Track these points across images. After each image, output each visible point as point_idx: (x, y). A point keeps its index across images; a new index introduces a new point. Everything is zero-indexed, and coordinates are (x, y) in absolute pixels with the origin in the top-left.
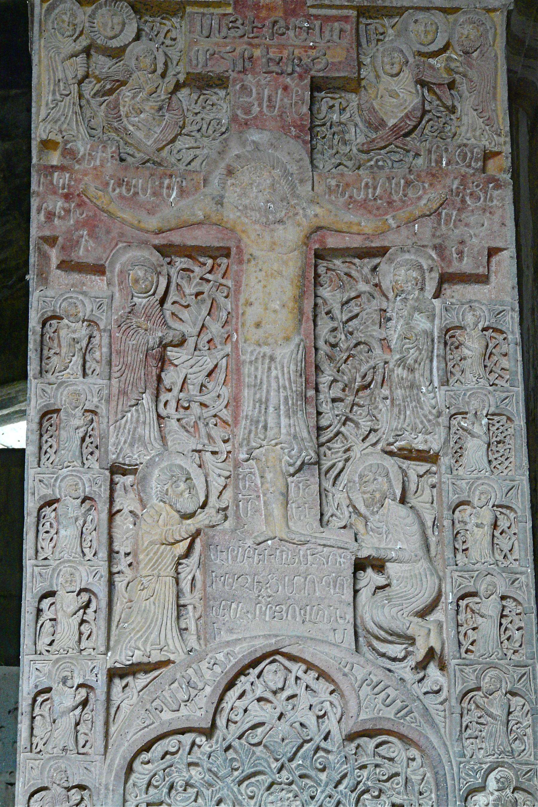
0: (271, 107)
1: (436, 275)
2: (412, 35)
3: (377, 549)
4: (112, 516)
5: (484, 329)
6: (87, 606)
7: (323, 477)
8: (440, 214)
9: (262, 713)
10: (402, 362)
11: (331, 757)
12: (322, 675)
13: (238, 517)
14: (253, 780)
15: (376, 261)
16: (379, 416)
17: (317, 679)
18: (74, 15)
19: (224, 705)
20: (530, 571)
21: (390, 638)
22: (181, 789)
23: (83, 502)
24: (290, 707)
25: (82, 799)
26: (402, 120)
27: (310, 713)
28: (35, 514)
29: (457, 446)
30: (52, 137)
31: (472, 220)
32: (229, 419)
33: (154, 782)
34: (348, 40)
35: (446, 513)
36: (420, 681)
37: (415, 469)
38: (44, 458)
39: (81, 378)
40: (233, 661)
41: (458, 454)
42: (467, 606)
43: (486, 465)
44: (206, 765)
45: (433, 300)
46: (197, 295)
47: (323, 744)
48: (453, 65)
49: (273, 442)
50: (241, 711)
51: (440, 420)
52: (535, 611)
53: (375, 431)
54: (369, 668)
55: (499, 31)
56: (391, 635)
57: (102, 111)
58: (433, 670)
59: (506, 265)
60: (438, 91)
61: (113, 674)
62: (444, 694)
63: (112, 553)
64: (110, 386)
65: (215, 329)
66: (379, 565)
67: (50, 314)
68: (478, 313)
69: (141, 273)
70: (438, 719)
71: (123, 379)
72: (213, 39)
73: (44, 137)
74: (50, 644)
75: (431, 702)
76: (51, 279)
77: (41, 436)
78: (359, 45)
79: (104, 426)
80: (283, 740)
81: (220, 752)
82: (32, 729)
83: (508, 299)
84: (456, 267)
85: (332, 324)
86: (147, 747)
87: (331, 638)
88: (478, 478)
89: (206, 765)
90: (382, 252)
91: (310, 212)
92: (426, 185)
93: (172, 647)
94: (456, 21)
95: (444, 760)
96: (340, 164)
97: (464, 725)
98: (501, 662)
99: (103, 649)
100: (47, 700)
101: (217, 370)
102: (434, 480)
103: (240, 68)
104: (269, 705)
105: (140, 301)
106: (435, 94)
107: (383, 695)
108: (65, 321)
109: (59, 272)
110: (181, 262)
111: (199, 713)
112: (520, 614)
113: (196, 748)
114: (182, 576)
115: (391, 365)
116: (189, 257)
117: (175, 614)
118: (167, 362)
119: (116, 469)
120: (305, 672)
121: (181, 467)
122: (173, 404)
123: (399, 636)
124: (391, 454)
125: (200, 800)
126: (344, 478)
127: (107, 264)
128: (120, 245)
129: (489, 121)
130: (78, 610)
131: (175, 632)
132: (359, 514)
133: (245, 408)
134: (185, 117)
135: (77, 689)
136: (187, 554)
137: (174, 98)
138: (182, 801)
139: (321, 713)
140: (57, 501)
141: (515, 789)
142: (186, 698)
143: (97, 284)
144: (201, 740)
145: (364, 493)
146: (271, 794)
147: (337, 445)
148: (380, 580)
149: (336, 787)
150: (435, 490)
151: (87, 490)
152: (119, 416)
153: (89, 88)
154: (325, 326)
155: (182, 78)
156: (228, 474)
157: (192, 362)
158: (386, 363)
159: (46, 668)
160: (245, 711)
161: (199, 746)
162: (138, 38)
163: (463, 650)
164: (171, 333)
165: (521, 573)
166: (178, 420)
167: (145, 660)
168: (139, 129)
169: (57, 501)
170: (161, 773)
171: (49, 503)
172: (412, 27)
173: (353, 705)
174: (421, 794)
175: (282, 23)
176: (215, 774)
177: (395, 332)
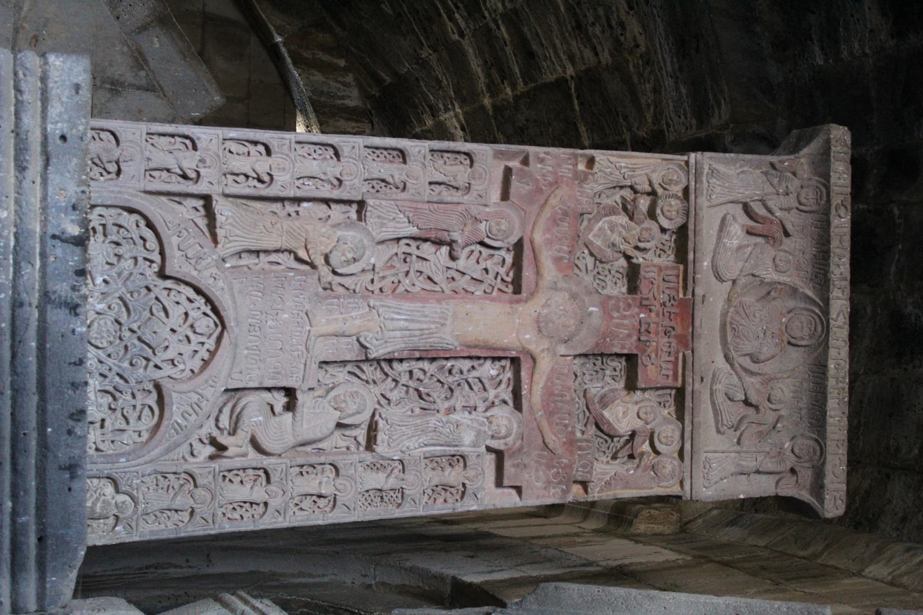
0: (618, 326)
1: (502, 447)
2: (665, 427)
3: (303, 406)
4: (327, 202)
5: (464, 485)
7: (355, 364)
9: (176, 316)
11: (141, 371)
12: (206, 363)
13: (326, 298)
14: (124, 309)
15: (511, 403)
16: (399, 406)
17: (203, 360)
18: (677, 183)
20: (286, 525)
21: (234, 416)
22: (116, 251)
23: (338, 179)
24: (181, 338)
25: (109, 173)
27: (176, 354)
28: (329, 142)
29: (378, 465)
30: (597, 165)
31: (541, 473)
32: (398, 291)
33: (122, 230)
34: (662, 382)
35: (330, 459)
36: (201, 440)
37: (361, 434)
38: (369, 151)
39: (429, 180)
40: (218, 293)
41: (374, 467)
42: (259, 476)
43: (366, 489)
44: (136, 271)
45: (484, 447)
46: (486, 270)
47: (151, 364)
48: (645, 457)
49: (382, 325)
50: (177, 299)
52: (256, 529)
53: (389, 404)
54: (212, 400)
55: (668, 490)
56: (237, 417)
58: (210, 450)
59: (507, 500)
60: (627, 447)
61: (207, 199)
62: (191, 459)
63: (298, 200)
64: (424, 202)
65: (463, 282)
66: (290, 406)
67: (474, 158)
69: (503, 227)
70: (172, 455)
71: (427, 212)
72: (662, 284)
73: (597, 159)
74: (230, 152)
75: (185, 448)
78: (657, 389)
79: (394, 197)
81: (144, 283)
82: (164, 135)
83: (486, 502)
85: (465, 370)
86: (150, 225)
87: (235, 370)
88: (356, 482)
89: (136, 271)
90: (518, 406)
94: (674, 458)
95: (141, 460)
96: (576, 376)
97: (167, 475)
98: (217, 505)
99: (227, 191)
100: (187, 147)
101: (433, 285)
102: (353, 448)
103: (645, 302)
104: (182, 321)
105: (483, 226)
106: (625, 445)
108: (469, 170)
109: (503, 167)
110: (509, 259)
111: (177, 266)
112: (253, 516)
113: (148, 263)
114: (281, 255)
115: (438, 415)
116: (513, 264)
117: (253, 248)
119: (361, 205)
120: (208, 350)
121: (362, 256)
122: (408, 250)
123: (236, 423)
124: (373, 415)
125: (107, 267)
126: (355, 379)
127: (509, 202)
128: (523, 213)
129: (608, 483)
130: (257, 174)
131: (239, 249)
132: (328, 391)
134: (607, 263)
135: (196, 171)
137: (621, 255)
138: (107, 252)
139: (176, 363)
140: (339, 160)
141: (117, 517)
142: (189, 256)
143: (495, 195)
145: (345, 396)
147: (379, 375)
148: (278, 408)
149: (118, 374)
150: (345, 449)
151: (347, 183)
152: (402, 209)
153: (628, 193)
154: (466, 365)
155: (634, 261)
156: (357, 291)
157: (439, 266)
158: (438, 411)
159: (214, 146)
160: (178, 303)
161: (150, 266)
163: (226, 474)
164: (459, 249)
165: (285, 517)
166: (396, 254)
167: (218, 224)
169: (339, 160)
170: (129, 236)
171: (337, 154)
172: (671, 427)
173: (184, 387)
174: (113, 442)
176: (127, 279)
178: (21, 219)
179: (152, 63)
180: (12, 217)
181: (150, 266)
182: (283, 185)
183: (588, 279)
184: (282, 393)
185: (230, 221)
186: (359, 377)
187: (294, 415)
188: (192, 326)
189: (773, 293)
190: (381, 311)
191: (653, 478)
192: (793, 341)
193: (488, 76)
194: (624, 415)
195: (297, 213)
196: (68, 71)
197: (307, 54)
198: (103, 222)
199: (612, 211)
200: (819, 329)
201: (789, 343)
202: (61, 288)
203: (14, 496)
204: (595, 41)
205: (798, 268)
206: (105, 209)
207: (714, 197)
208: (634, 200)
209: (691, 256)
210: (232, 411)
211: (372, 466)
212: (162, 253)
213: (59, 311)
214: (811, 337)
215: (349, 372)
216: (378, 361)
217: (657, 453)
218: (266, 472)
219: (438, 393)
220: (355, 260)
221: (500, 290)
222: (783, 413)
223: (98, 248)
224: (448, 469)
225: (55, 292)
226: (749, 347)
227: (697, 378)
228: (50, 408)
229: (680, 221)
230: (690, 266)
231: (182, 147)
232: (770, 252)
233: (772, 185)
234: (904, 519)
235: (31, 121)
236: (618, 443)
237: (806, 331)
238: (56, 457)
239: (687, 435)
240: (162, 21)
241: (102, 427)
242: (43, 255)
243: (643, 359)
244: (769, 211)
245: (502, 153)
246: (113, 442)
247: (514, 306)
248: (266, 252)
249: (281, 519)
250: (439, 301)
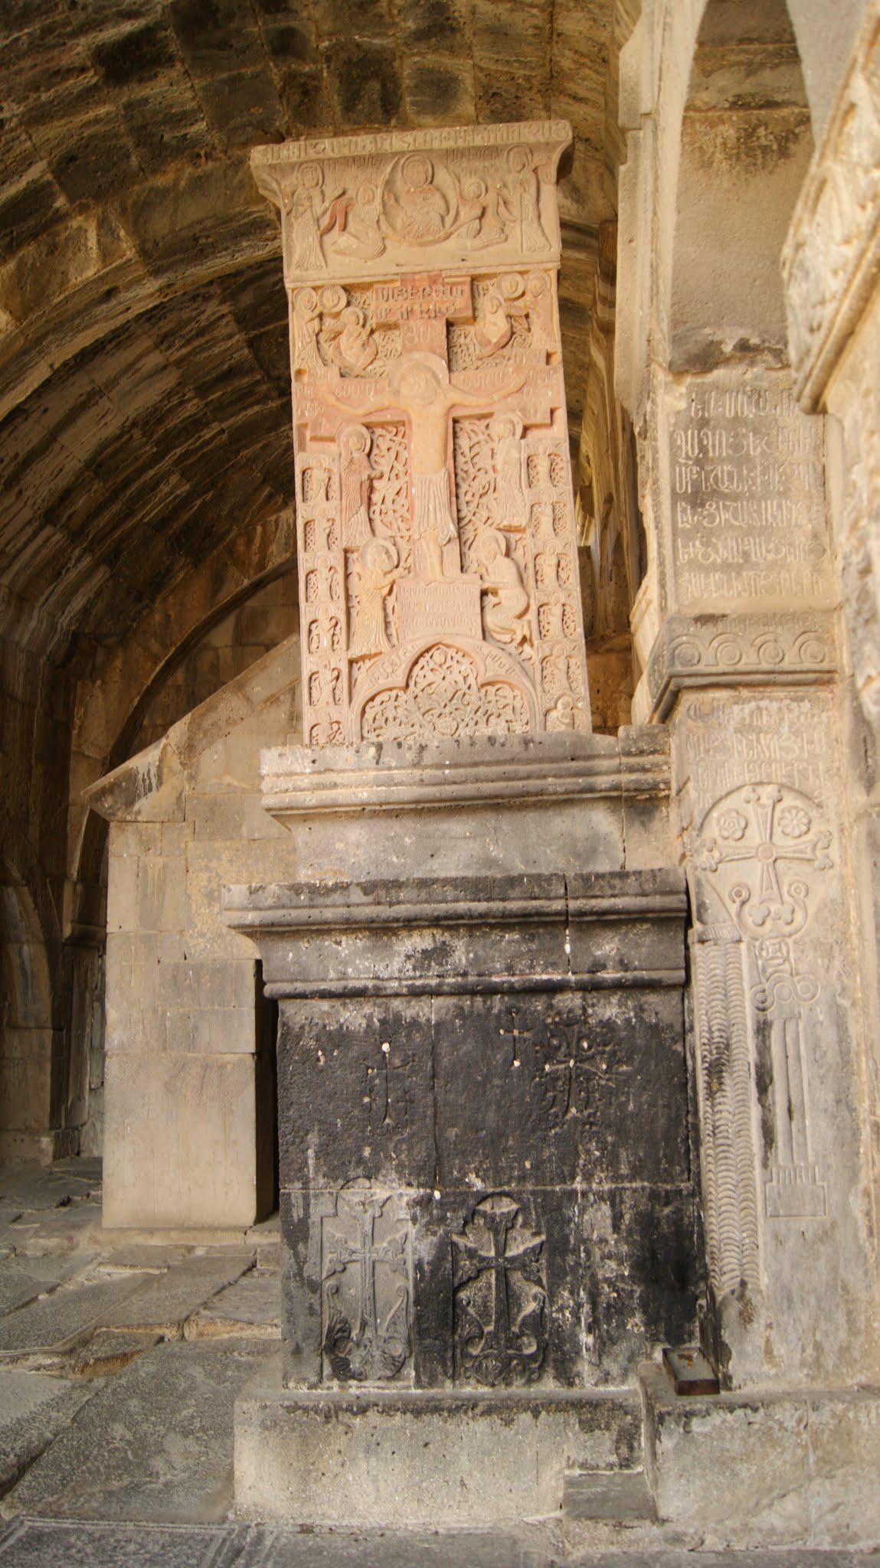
4: (347, 576)
15: (487, 421)
20: (579, 589)
41: (537, 527)
58: (526, 647)
63: (348, 597)
65: (398, 467)
70: (530, 673)
86: (372, 699)
90: (490, 415)
105: (356, 455)
110: (379, 431)
124: (499, 530)
143: (333, 447)
144: (401, 693)
147: (470, 527)
153: (322, 337)
154: (461, 459)
175: (428, 289)
177: (499, 462)
179: (274, 691)
182: (338, 610)
193: (251, 405)
194: (493, 325)
196: (271, 761)
197: (256, 559)
202: (410, 756)
203: (545, 777)
204: (213, 318)
212: (390, 689)
214: (424, 163)
217: (523, 294)
219: (482, 480)
220: (387, 552)
223: (390, 732)
224: (539, 468)
228: (488, 758)
229: (342, 292)
234: (595, 20)
235: (305, 782)
236: (518, 328)
237: (421, 168)
239: (509, 269)
240: (240, 687)
242: (390, 768)
243: (449, 315)
248: (386, 616)
250: (412, 485)
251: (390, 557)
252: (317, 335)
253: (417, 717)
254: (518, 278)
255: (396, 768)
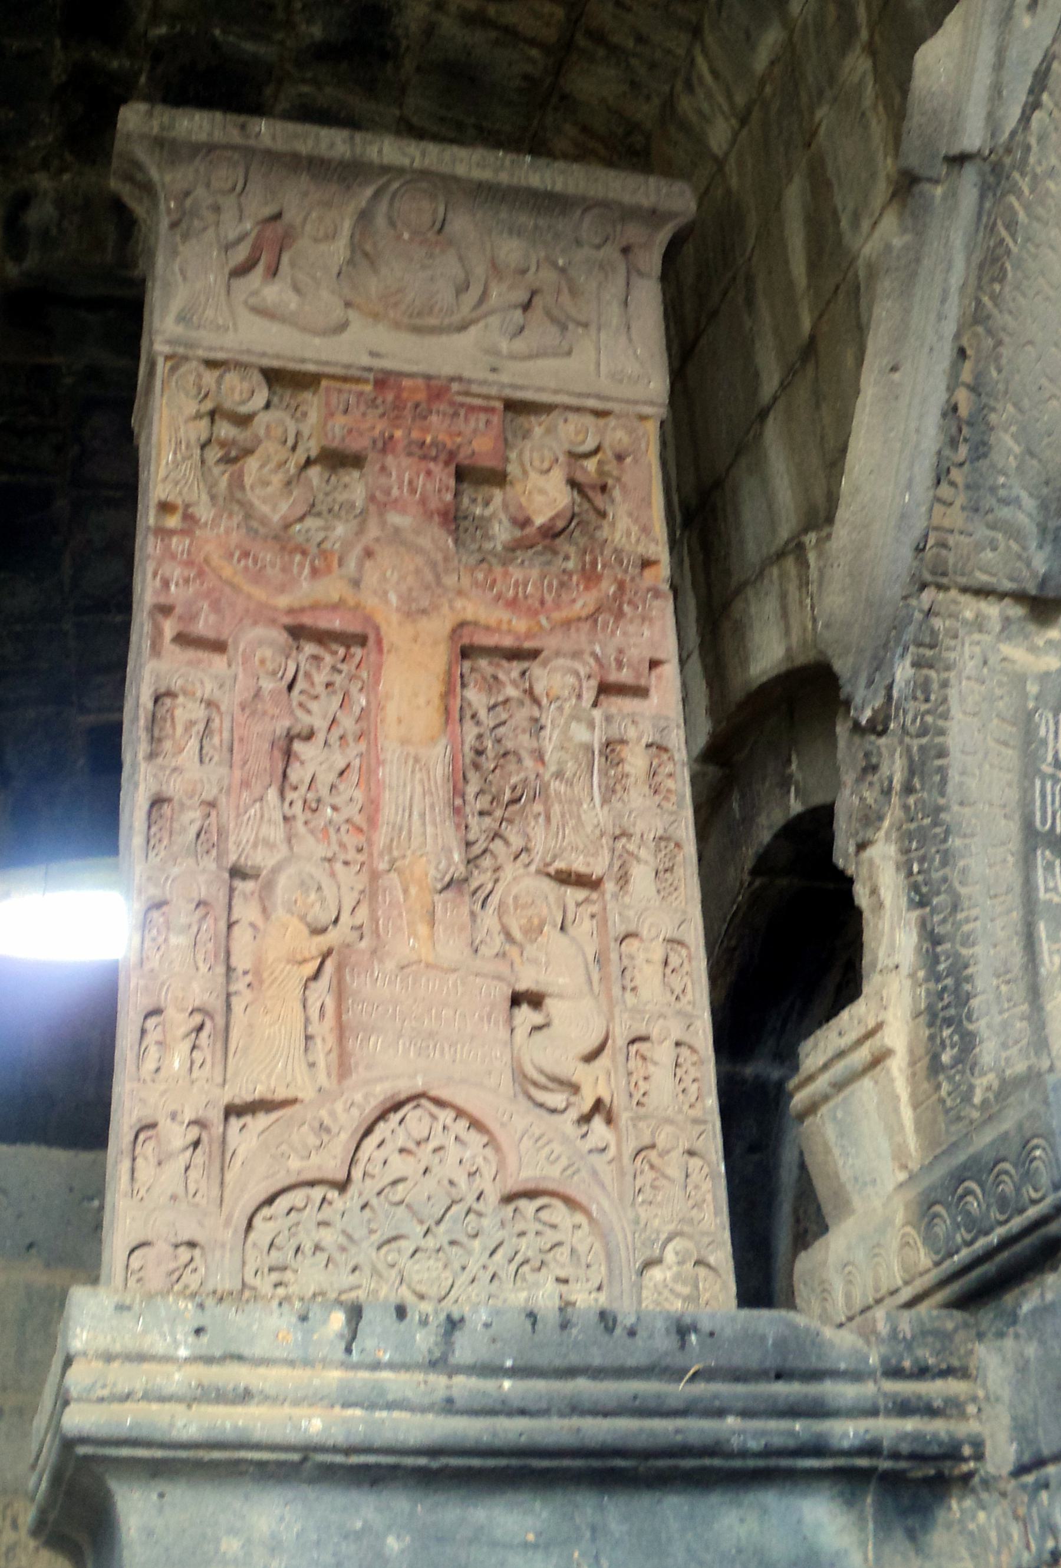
0: (413, 490)
1: (594, 683)
4: (230, 926)
5: (649, 746)
6: (200, 1028)
8: (596, 621)
10: (559, 775)
11: (485, 1222)
12: (475, 1124)
14: (394, 1245)
15: (525, 665)
18: (199, 376)
19: (360, 1154)
24: (437, 1160)
25: (192, 1260)
26: (553, 519)
29: (621, 872)
31: (631, 629)
37: (573, 895)
38: (152, 855)
40: (373, 1102)
41: (623, 879)
46: (328, 685)
47: (475, 1206)
49: (419, 853)
51: (604, 840)
57: (224, 482)
58: (598, 1122)
62: (612, 1152)
65: (347, 723)
66: (535, 1000)
68: (641, 727)
70: (608, 1181)
73: (163, 497)
75: (595, 1158)
76: (163, 653)
77: (149, 827)
80: (429, 1198)
82: (133, 1171)
84: (614, 677)
86: (270, 1201)
89: (339, 1224)
90: (534, 654)
91: (459, 604)
92: (582, 587)
93: (300, 1082)
94: (606, 425)
99: (220, 1080)
100: (150, 1138)
102: (594, 908)
103: (380, 444)
104: (410, 1159)
107: (546, 1151)
108: (181, 699)
110: (310, 648)
113: (325, 1205)
114: (310, 1002)
118: (292, 759)
122: (298, 806)
124: (548, 875)
126: (494, 900)
127: (230, 640)
129: (646, 530)
131: (304, 1066)
133: (386, 811)
136: (316, 976)
137: (303, 475)
142: (318, 1143)
144: (333, 1194)
146: (417, 1262)
147: (487, 862)
148: (537, 1018)
152: (242, 810)
155: (314, 453)
162: (268, 406)
167: (269, 1096)
168: (264, 502)
170: (286, 1232)
173: (512, 1160)
174: (588, 1266)
177: (550, 740)
178: (321, 1399)
180: (318, 1410)
181: (330, 1203)
183: (340, 529)
184: (516, 1011)
185: (263, 1077)
186: (491, 892)
187: (550, 995)
188: (418, 1143)
189: (368, 247)
190: (396, 853)
191: (636, 461)
192: (438, 225)
195: (245, 973)
198: (266, 1270)
199: (237, 482)
200: (424, 185)
201: (440, 231)
202: (424, 1341)
205: (328, 205)
206: (247, 1268)
207: (221, 322)
208: (223, 444)
209: (311, 368)
210: (544, 1088)
211: (622, 882)
212: (312, 1184)
213: (457, 1346)
214: (433, 197)
215: (483, 906)
216: (469, 862)
217: (597, 451)
218: (633, 1042)
220: (319, 888)
221: (358, 666)
222: (542, 254)
225: (430, 1351)
226: (445, 295)
227: (492, 377)
228: (597, 1361)
229: (257, 377)
230: (327, 370)
231: (150, 1145)
232: (303, 243)
233: (205, 229)
237: (426, 204)
238: (666, 1354)
241: (566, 1281)
242: (376, 1366)
244: (240, 239)
245: (154, 646)
246: (588, 1266)
247: (386, 647)
249: (698, 1024)
251: (323, 900)
252: (203, 447)
253: (365, 1253)
254: (589, 420)
255: (391, 1366)
